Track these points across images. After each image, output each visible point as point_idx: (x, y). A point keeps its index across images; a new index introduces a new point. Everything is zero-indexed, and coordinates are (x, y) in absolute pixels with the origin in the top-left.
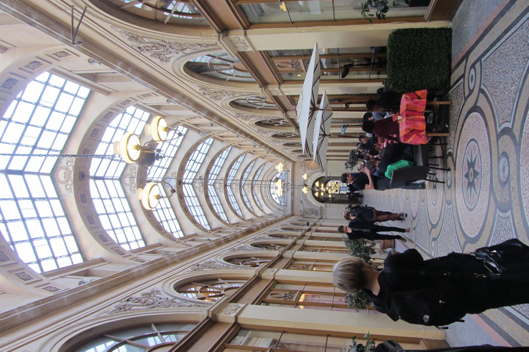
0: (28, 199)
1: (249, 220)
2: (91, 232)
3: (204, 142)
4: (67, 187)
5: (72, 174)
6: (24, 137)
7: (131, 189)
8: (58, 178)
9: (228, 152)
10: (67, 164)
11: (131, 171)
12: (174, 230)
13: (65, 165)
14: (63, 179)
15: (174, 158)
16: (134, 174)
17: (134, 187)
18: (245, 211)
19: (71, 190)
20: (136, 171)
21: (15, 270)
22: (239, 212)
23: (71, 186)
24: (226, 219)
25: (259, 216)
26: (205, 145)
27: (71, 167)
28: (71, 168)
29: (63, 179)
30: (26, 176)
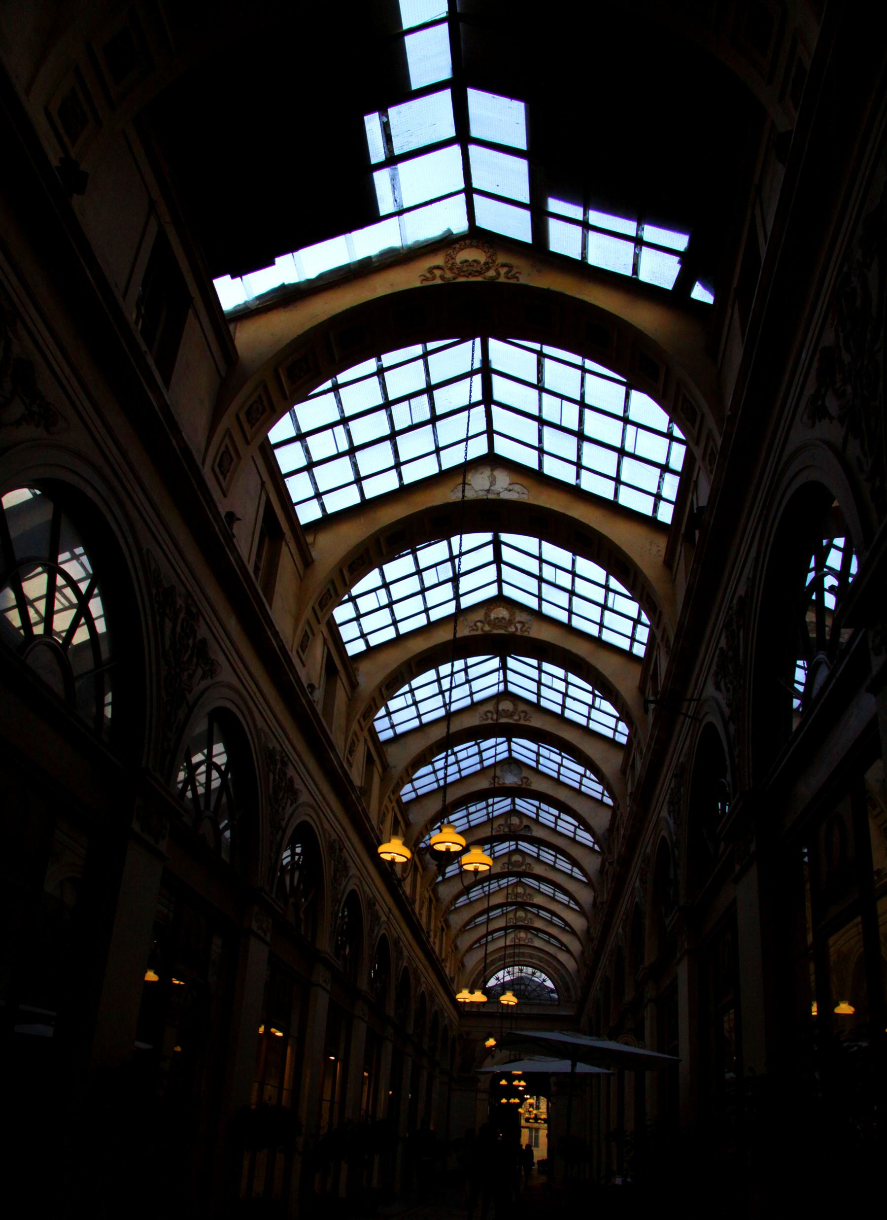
0: (434, 427)
1: (446, 921)
2: (402, 664)
3: (618, 719)
4: (479, 624)
5: (502, 632)
6: (553, 569)
7: (489, 711)
8: (496, 607)
9: (599, 796)
10: (519, 622)
11: (523, 712)
12: (417, 784)
13: (518, 619)
14: (493, 616)
15: (554, 830)
16: (516, 717)
17: (492, 719)
18: (466, 915)
19: (473, 630)
20: (522, 722)
21: (269, 399)
22: (462, 901)
23: (482, 629)
24: (457, 905)
25: (465, 959)
26: (612, 722)
27: (514, 630)
28: (512, 629)
29: (493, 616)
30: (494, 566)
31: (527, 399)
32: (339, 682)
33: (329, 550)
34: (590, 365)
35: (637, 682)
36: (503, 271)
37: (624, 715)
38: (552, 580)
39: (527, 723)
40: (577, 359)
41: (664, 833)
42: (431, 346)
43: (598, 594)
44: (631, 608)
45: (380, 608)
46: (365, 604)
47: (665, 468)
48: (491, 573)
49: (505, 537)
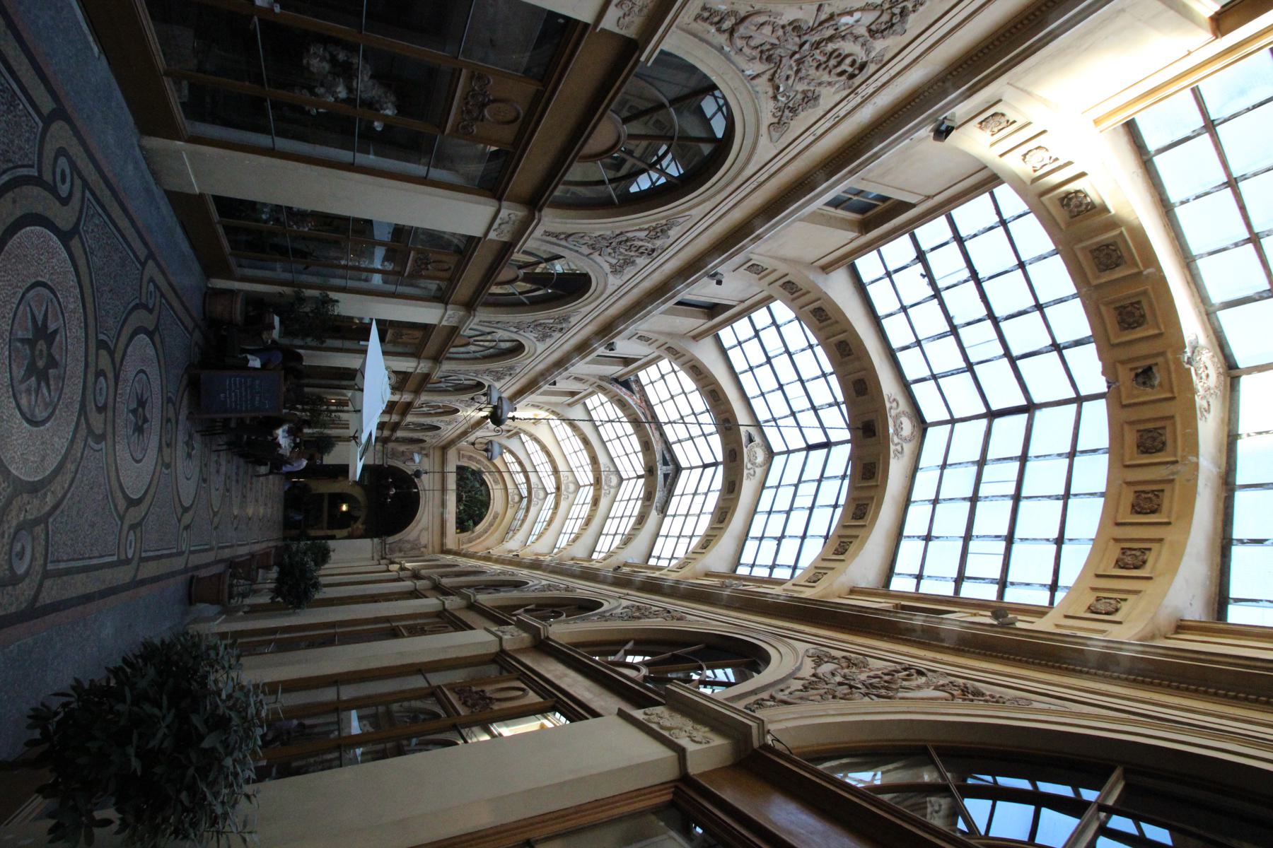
31: (813, 472)
32: (702, 321)
33: (706, 354)
34: (839, 511)
35: (630, 561)
36: (899, 448)
37: (610, 554)
38: (984, 479)
39: (892, 455)
40: (842, 501)
41: (606, 606)
42: (843, 407)
43: (688, 531)
44: (680, 553)
45: (669, 389)
46: (671, 378)
47: (772, 568)
48: (796, 442)
49: (721, 468)
